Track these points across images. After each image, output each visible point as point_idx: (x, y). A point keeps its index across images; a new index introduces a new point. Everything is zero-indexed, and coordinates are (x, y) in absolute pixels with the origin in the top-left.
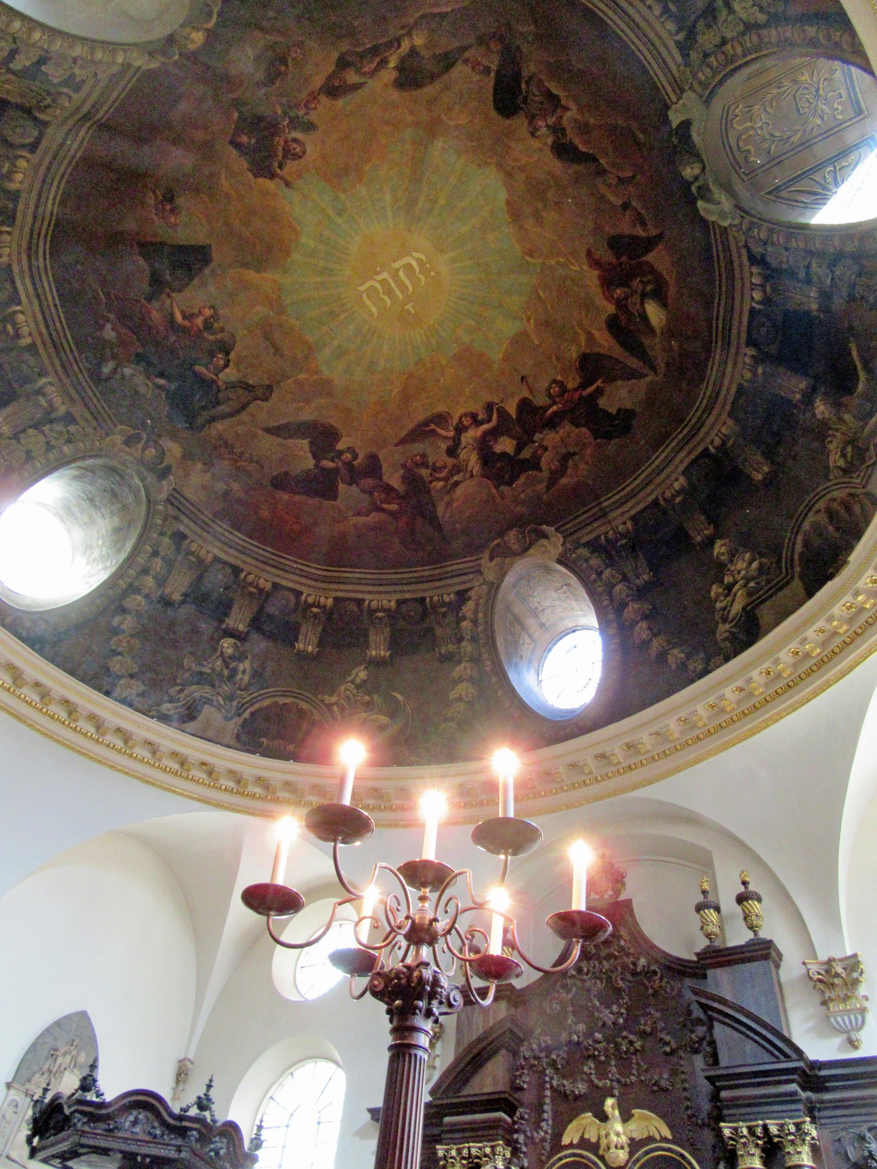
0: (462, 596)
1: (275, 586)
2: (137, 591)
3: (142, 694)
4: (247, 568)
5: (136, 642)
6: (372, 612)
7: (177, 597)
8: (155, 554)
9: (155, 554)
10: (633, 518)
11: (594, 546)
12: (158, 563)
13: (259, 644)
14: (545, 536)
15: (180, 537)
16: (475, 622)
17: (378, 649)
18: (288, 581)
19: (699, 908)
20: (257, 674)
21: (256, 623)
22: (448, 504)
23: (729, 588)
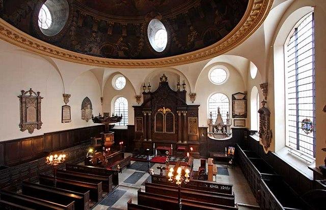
0: (141, 25)
1: (101, 20)
2: (72, 26)
3: (80, 48)
4: (94, 16)
5: (75, 37)
6: (122, 26)
7: (81, 25)
8: (74, 17)
9: (74, 17)
10: (177, 16)
11: (168, 19)
12: (75, 18)
13: (100, 34)
14: (158, 15)
15: (77, 11)
16: (144, 30)
17: (124, 34)
18: (104, 19)
19: (177, 85)
20: (101, 40)
21: (99, 29)
22: (138, 3)
23: (192, 36)
